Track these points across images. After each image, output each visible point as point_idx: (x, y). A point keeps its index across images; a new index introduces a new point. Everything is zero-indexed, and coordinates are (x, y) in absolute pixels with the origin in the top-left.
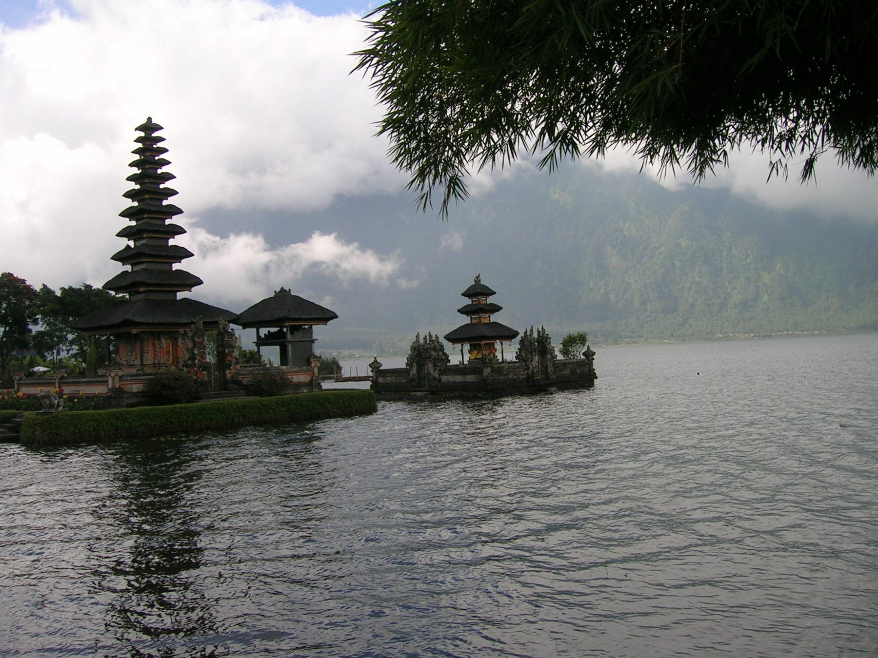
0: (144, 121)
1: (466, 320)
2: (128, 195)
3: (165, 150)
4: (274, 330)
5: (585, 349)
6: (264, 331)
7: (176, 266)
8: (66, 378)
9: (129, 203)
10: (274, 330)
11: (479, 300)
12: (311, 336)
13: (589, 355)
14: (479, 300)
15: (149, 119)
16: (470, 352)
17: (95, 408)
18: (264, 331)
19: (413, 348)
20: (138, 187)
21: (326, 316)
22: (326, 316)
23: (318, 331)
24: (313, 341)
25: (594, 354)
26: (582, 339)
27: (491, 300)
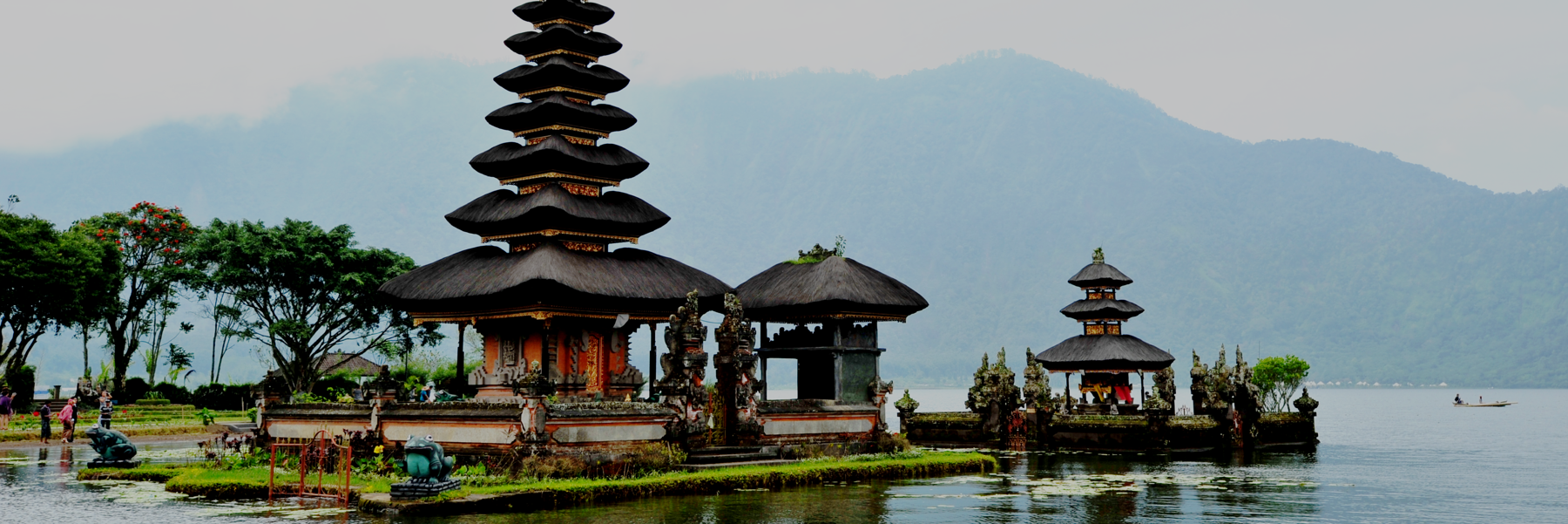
1: (1076, 328)
2: (514, 44)
4: (789, 327)
5: (1298, 394)
6: (773, 329)
8: (398, 407)
10: (789, 327)
11: (1101, 299)
12: (875, 344)
13: (1307, 408)
14: (1101, 299)
17: (556, 475)
18: (773, 329)
19: (980, 376)
21: (905, 303)
22: (905, 303)
24: (878, 353)
25: (1316, 405)
26: (1293, 372)
27: (1121, 294)
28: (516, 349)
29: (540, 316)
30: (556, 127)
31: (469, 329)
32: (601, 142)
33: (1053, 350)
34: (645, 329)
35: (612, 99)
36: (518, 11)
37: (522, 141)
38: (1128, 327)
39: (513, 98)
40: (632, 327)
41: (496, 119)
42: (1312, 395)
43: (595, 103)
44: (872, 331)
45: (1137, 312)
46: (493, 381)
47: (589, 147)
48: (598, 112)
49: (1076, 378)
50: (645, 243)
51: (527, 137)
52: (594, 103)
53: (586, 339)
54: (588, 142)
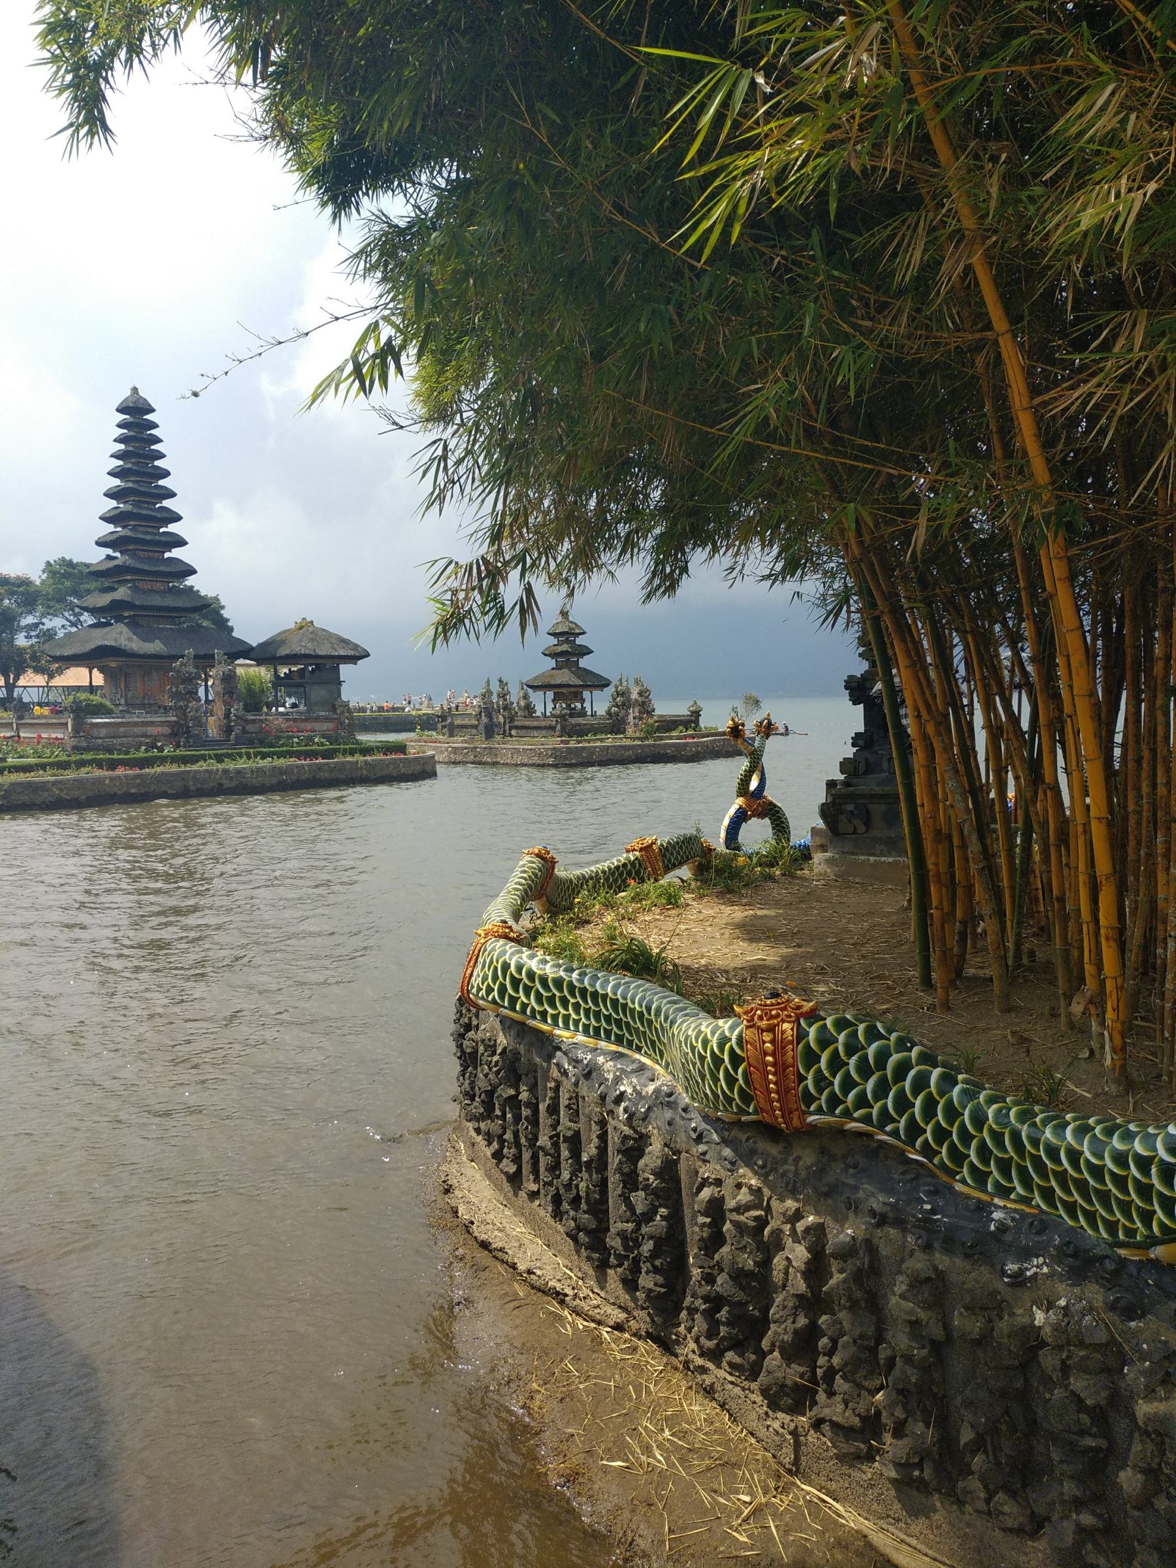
1: (552, 663)
2: (110, 495)
6: (283, 671)
16: (554, 701)
18: (283, 671)
21: (357, 656)
22: (357, 656)
23: (345, 670)
27: (580, 641)
29: (113, 665)
30: (131, 547)
31: (95, 671)
32: (167, 555)
33: (535, 678)
35: (172, 528)
37: (118, 554)
38: (584, 662)
39: (111, 528)
41: (100, 543)
43: (162, 530)
45: (590, 652)
47: (158, 559)
48: (163, 539)
49: (550, 695)
51: (121, 553)
52: (162, 530)
53: (155, 675)
54: (156, 555)
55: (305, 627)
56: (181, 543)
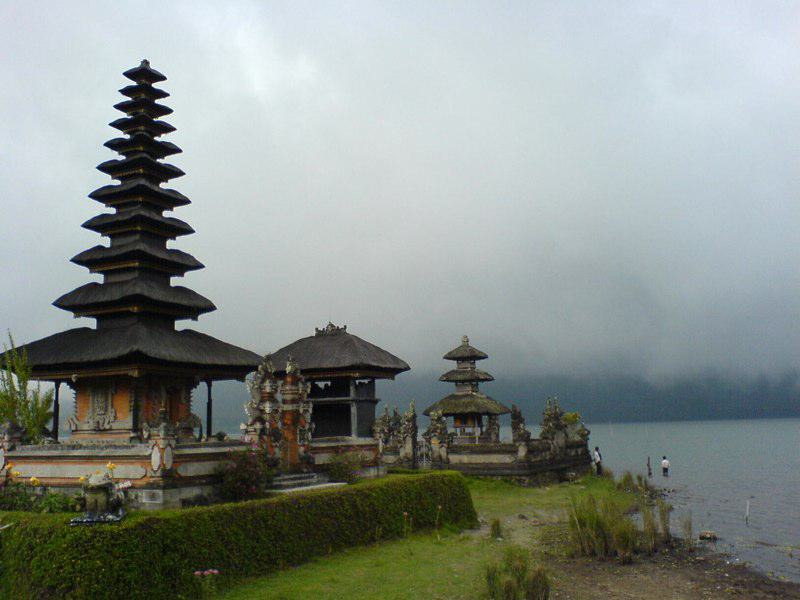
0: (137, 64)
2: (105, 168)
3: (168, 111)
7: (175, 281)
9: (107, 180)
12: (374, 396)
13: (585, 436)
15: (146, 62)
20: (123, 158)
23: (381, 385)
27: (480, 365)
28: (106, 400)
29: (135, 374)
34: (203, 385)
36: (108, 144)
40: (195, 385)
42: (588, 427)
44: (372, 384)
46: (86, 427)
50: (203, 324)
55: (333, 336)
56: (185, 230)
